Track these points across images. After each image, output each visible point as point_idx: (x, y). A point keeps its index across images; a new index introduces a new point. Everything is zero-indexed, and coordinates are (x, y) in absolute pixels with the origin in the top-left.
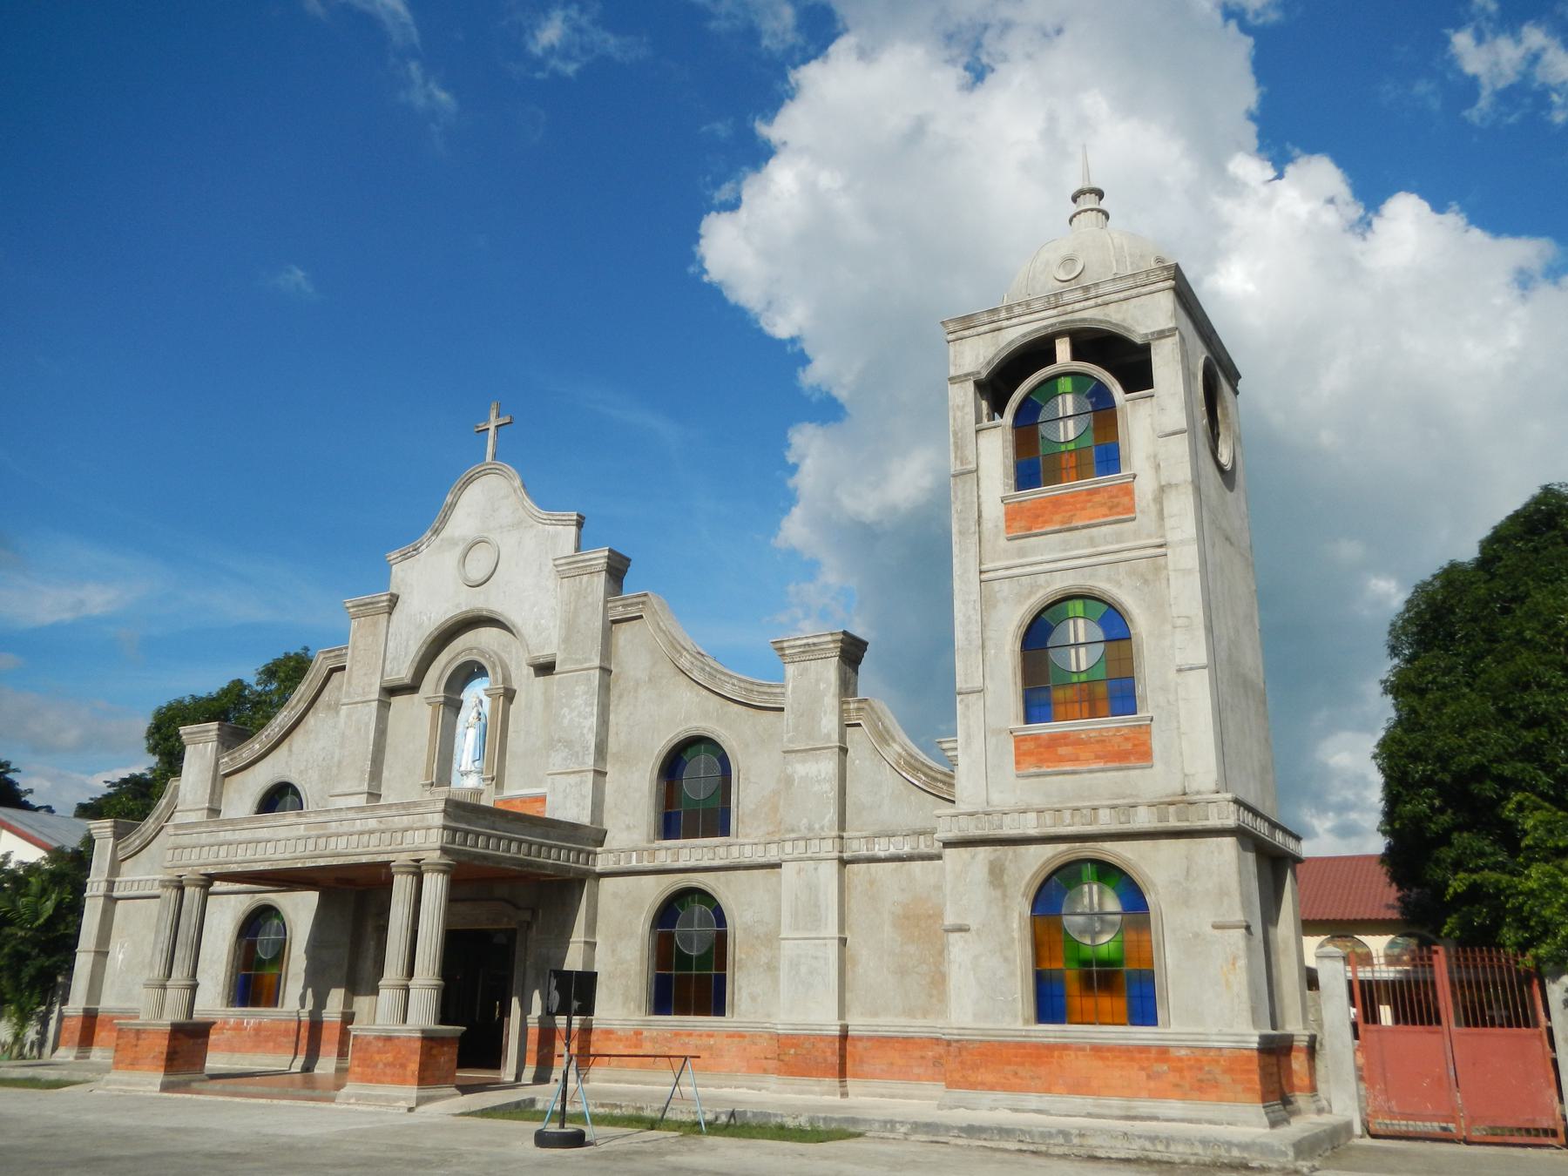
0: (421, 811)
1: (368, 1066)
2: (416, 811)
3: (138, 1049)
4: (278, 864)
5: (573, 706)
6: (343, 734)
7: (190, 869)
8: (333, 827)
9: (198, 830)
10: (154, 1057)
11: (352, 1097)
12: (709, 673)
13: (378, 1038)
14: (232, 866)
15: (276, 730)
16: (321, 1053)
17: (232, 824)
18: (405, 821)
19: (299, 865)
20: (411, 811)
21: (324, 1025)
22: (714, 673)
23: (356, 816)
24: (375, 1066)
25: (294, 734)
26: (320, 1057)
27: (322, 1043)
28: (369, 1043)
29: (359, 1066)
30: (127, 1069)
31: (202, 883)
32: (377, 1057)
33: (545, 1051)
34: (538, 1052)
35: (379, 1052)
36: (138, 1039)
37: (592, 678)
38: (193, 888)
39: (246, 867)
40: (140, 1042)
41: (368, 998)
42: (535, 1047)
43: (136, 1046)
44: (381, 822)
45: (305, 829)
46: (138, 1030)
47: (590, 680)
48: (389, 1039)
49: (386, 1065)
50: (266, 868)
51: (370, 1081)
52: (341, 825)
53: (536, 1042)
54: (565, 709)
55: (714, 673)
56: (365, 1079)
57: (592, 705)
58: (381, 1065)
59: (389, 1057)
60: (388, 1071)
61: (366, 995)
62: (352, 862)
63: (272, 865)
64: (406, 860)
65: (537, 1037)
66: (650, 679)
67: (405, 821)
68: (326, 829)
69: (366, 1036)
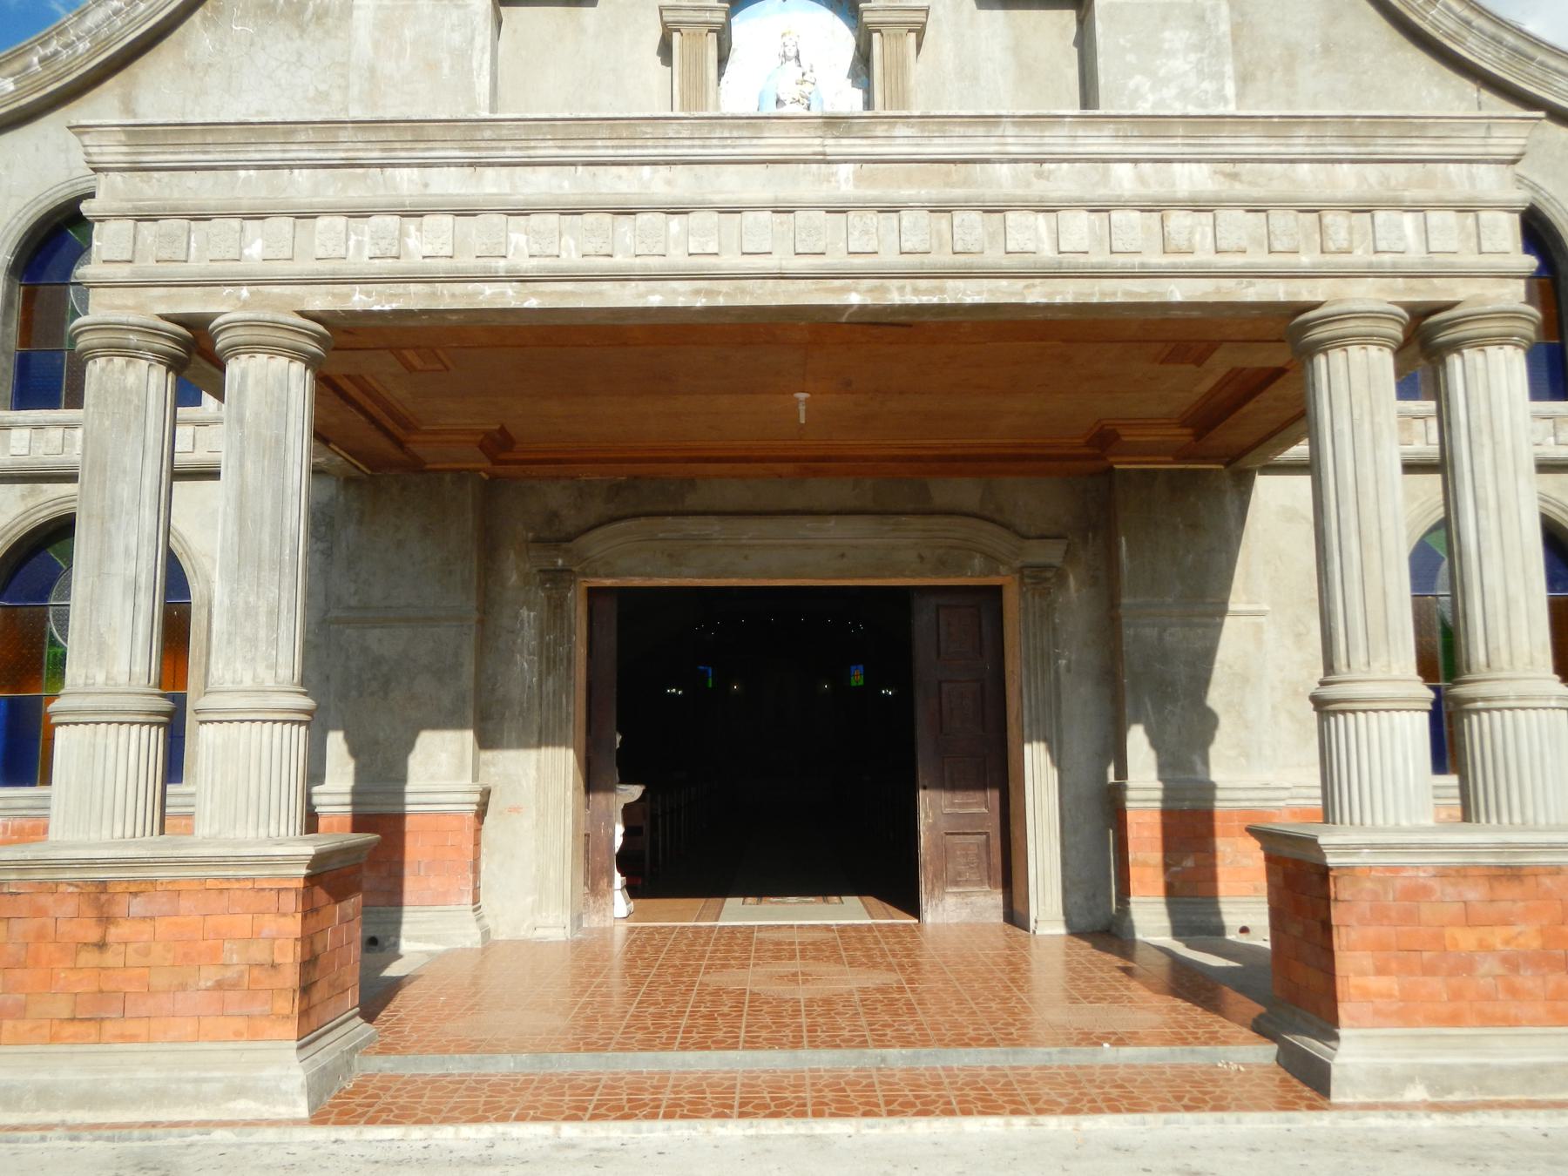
0: (1424, 148)
1: (1429, 970)
2: (1402, 150)
3: (110, 958)
4: (743, 291)
5: (1162, 73)
6: (372, 70)
7: (245, 292)
8: (1004, 180)
9: (275, 153)
10: (219, 986)
11: (1408, 1080)
12: (1515, 50)
13: (1443, 873)
14: (488, 289)
15: (82, 47)
16: (408, 897)
17: (466, 142)
18: (1349, 180)
19: (855, 299)
20: (1381, 148)
21: (410, 824)
22: (1530, 50)
23: (1117, 148)
24: (1466, 966)
25: (137, 67)
26: (406, 909)
27: (408, 871)
28: (1416, 893)
29: (1381, 971)
30: (54, 1039)
31: (313, 347)
32: (1466, 939)
33: (1189, 863)
34: (1167, 866)
35: (1469, 919)
36: (105, 920)
37: (1209, 15)
38: (282, 361)
39: (564, 294)
40: (114, 933)
41: (531, 756)
42: (1156, 856)
43: (101, 946)
44: (1234, 176)
45: (859, 180)
46: (103, 885)
47: (1202, 18)
48: (1512, 874)
49: (1512, 963)
50: (681, 302)
51: (1454, 1020)
52: (1039, 175)
53: (1158, 843)
54: (1138, 78)
55: (1530, 50)
56: (1405, 1013)
57: (1218, 76)
58: (1489, 966)
59: (1527, 936)
60: (1527, 979)
61: (524, 744)
62: (1120, 299)
63: (709, 293)
64: (1380, 301)
65: (1157, 833)
66: (1327, 49)
67: (1349, 180)
68: (965, 183)
69: (1396, 869)
